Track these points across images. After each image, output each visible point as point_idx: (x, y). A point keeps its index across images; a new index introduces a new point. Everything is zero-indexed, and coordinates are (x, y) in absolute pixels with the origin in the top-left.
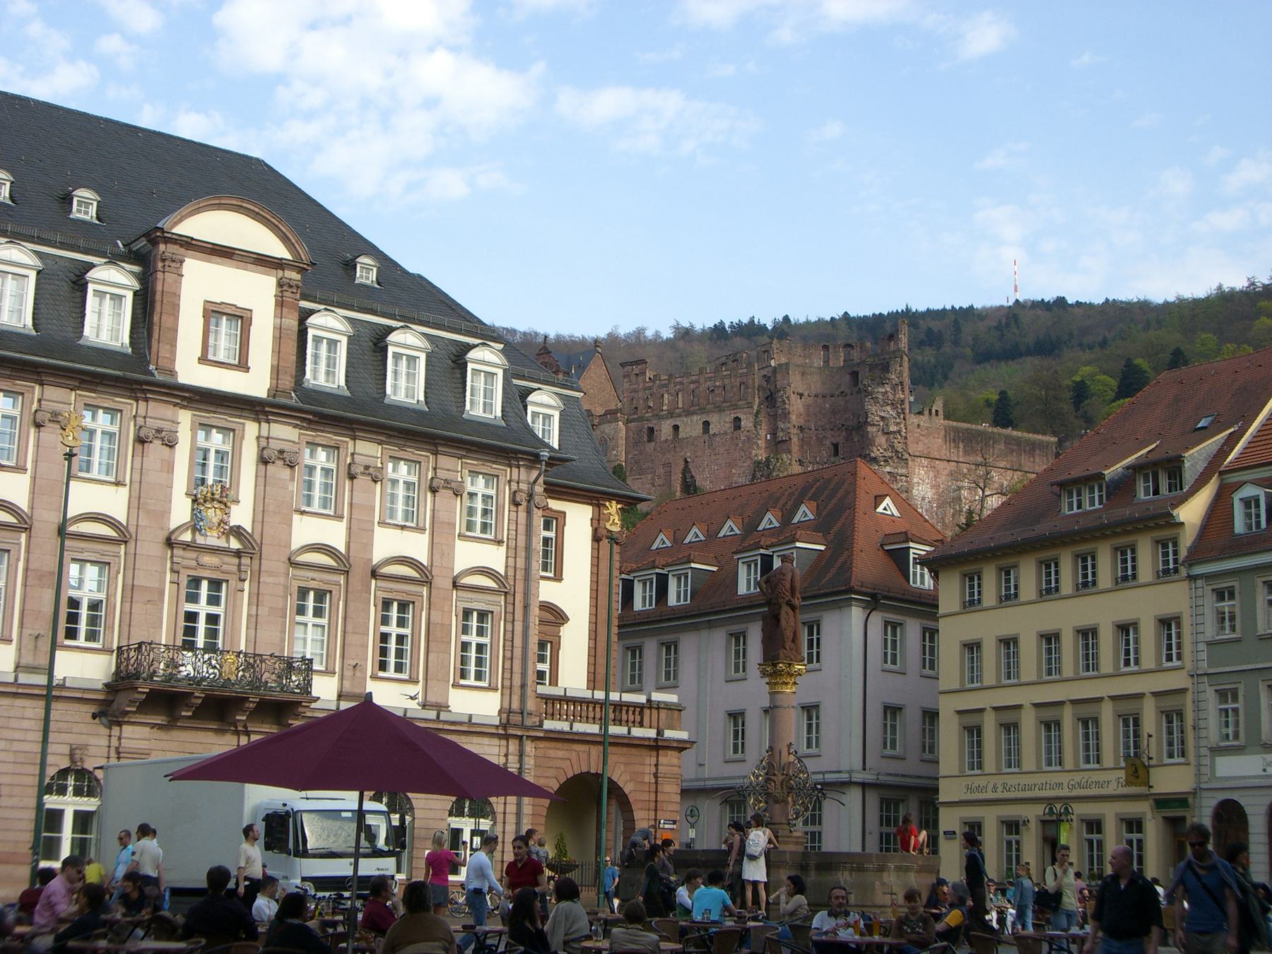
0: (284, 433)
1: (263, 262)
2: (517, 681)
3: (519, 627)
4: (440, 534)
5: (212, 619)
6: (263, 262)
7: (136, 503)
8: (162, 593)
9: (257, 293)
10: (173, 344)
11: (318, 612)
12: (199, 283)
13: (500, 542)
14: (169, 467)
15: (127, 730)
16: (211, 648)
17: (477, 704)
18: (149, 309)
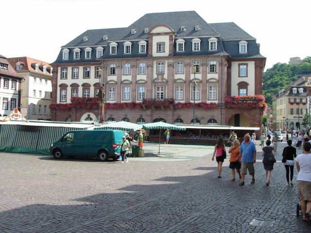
0: (171, 61)
1: (166, 34)
2: (220, 98)
3: (220, 88)
4: (204, 74)
5: (162, 93)
6: (166, 34)
7: (147, 77)
8: (152, 91)
9: (166, 39)
10: (152, 51)
11: (181, 90)
12: (156, 40)
13: (217, 73)
14: (152, 71)
15: (147, 112)
16: (162, 98)
17: (216, 102)
18: (149, 46)
